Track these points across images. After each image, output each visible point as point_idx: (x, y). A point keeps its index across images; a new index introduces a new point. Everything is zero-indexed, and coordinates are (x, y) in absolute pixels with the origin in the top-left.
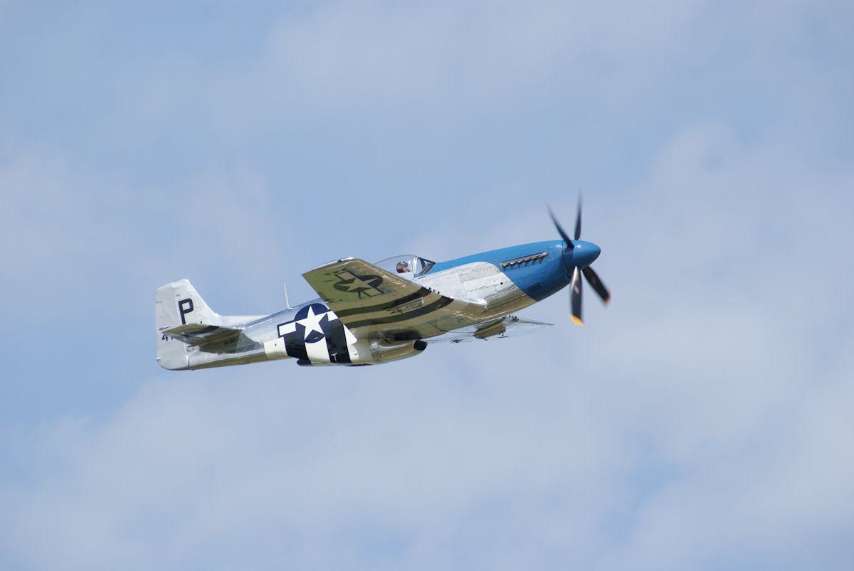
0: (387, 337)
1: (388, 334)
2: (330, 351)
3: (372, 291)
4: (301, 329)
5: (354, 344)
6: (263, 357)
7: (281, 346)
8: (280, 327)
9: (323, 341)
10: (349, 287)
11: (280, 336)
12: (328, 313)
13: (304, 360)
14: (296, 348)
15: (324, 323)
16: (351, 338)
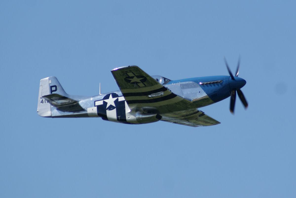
0: (144, 111)
1: (145, 110)
2: (118, 115)
3: (141, 85)
4: (105, 103)
5: (129, 113)
6: (87, 115)
7: (94, 110)
8: (96, 102)
9: (115, 110)
10: (131, 81)
11: (95, 106)
12: (119, 98)
13: (105, 117)
14: (102, 112)
15: (116, 102)
16: (128, 110)
